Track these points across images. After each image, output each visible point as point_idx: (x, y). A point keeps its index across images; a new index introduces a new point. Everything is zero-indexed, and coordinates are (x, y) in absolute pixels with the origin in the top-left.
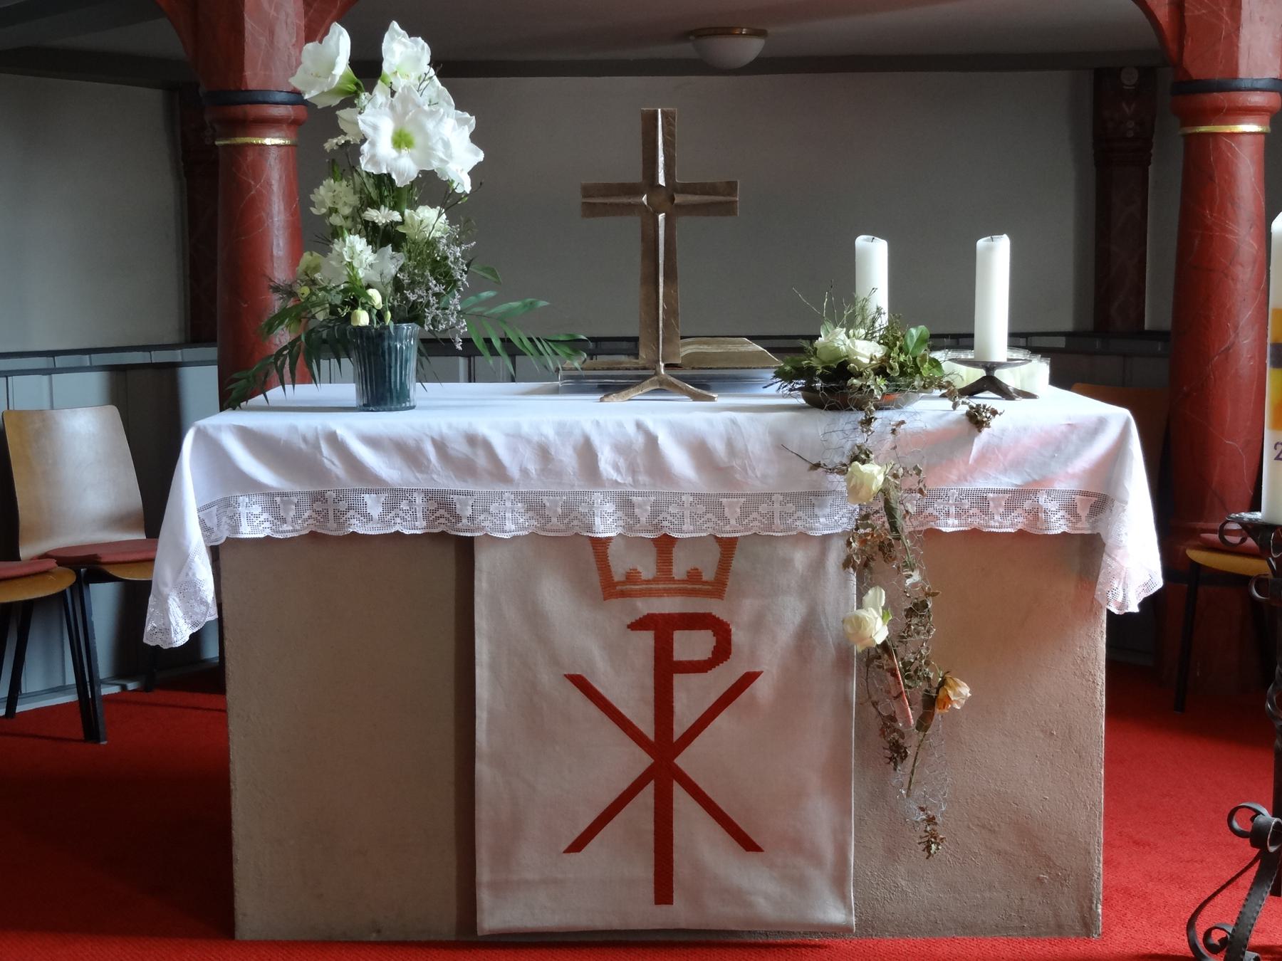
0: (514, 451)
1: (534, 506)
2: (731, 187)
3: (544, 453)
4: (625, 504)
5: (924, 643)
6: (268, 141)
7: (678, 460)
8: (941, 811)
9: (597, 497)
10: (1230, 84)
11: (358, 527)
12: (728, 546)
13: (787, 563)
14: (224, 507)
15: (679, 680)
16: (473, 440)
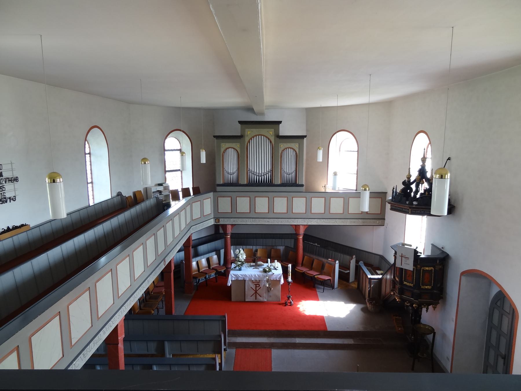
1: (249, 278)
2: (260, 257)
3: (249, 275)
4: (254, 278)
5: (270, 286)
7: (257, 276)
10: (299, 234)
11: (239, 279)
12: (260, 280)
15: (257, 287)
16: (246, 275)
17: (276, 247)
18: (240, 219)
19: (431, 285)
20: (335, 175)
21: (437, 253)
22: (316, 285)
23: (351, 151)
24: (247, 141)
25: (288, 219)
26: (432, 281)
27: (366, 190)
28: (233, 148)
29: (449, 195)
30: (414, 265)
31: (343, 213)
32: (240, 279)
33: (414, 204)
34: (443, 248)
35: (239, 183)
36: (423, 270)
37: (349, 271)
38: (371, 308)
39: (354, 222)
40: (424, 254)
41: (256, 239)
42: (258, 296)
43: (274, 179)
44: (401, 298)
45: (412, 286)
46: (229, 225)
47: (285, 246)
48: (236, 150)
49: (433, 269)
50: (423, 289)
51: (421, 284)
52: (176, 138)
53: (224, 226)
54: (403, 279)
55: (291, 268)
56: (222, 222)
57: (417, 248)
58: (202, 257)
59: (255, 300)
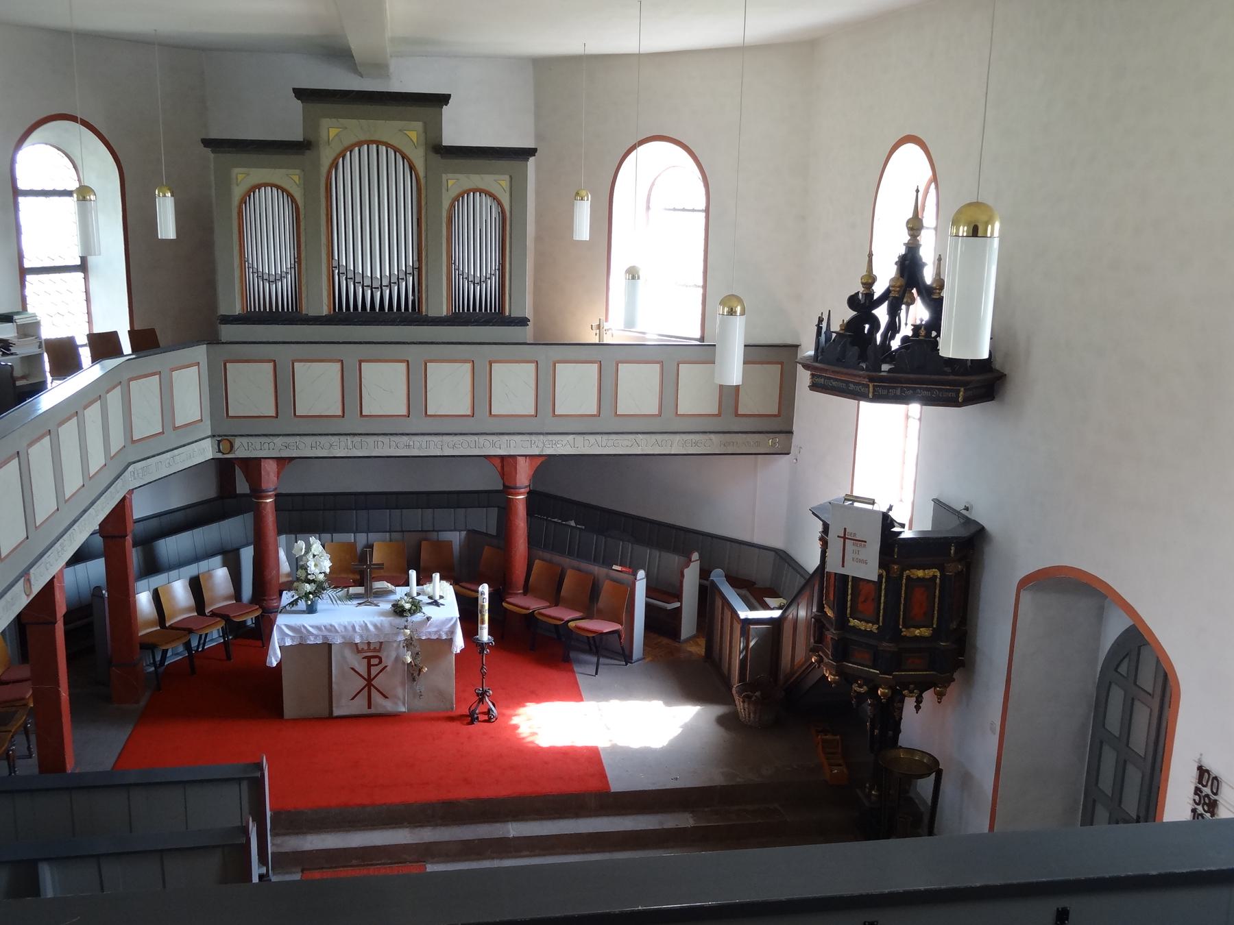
0: (339, 628)
1: (343, 637)
2: (383, 564)
3: (345, 627)
4: (361, 636)
6: (268, 501)
7: (371, 627)
8: (423, 690)
9: (356, 635)
10: (515, 488)
11: (309, 642)
12: (381, 643)
13: (393, 646)
14: (282, 639)
16: (331, 625)
17: (435, 533)
18: (309, 440)
19: (932, 626)
20: (633, 278)
21: (951, 528)
22: (573, 655)
23: (684, 210)
24: (326, 162)
25: (476, 438)
26: (936, 612)
27: (736, 312)
28: (278, 187)
29: (991, 339)
30: (882, 565)
31: (660, 415)
32: (311, 641)
33: (882, 370)
34: (967, 509)
35: (300, 312)
36: (908, 577)
37: (677, 605)
38: (749, 714)
39: (696, 444)
40: (910, 528)
41: (366, 508)
42: (376, 696)
43: (427, 299)
44: (839, 672)
45: (876, 631)
46: (271, 461)
47: (469, 531)
48: (289, 195)
49: (938, 574)
50: (908, 638)
51: (901, 623)
52: (59, 149)
53: (252, 466)
54: (848, 611)
55: (486, 596)
56: (243, 449)
57: (890, 509)
58: (174, 573)
59: (366, 711)
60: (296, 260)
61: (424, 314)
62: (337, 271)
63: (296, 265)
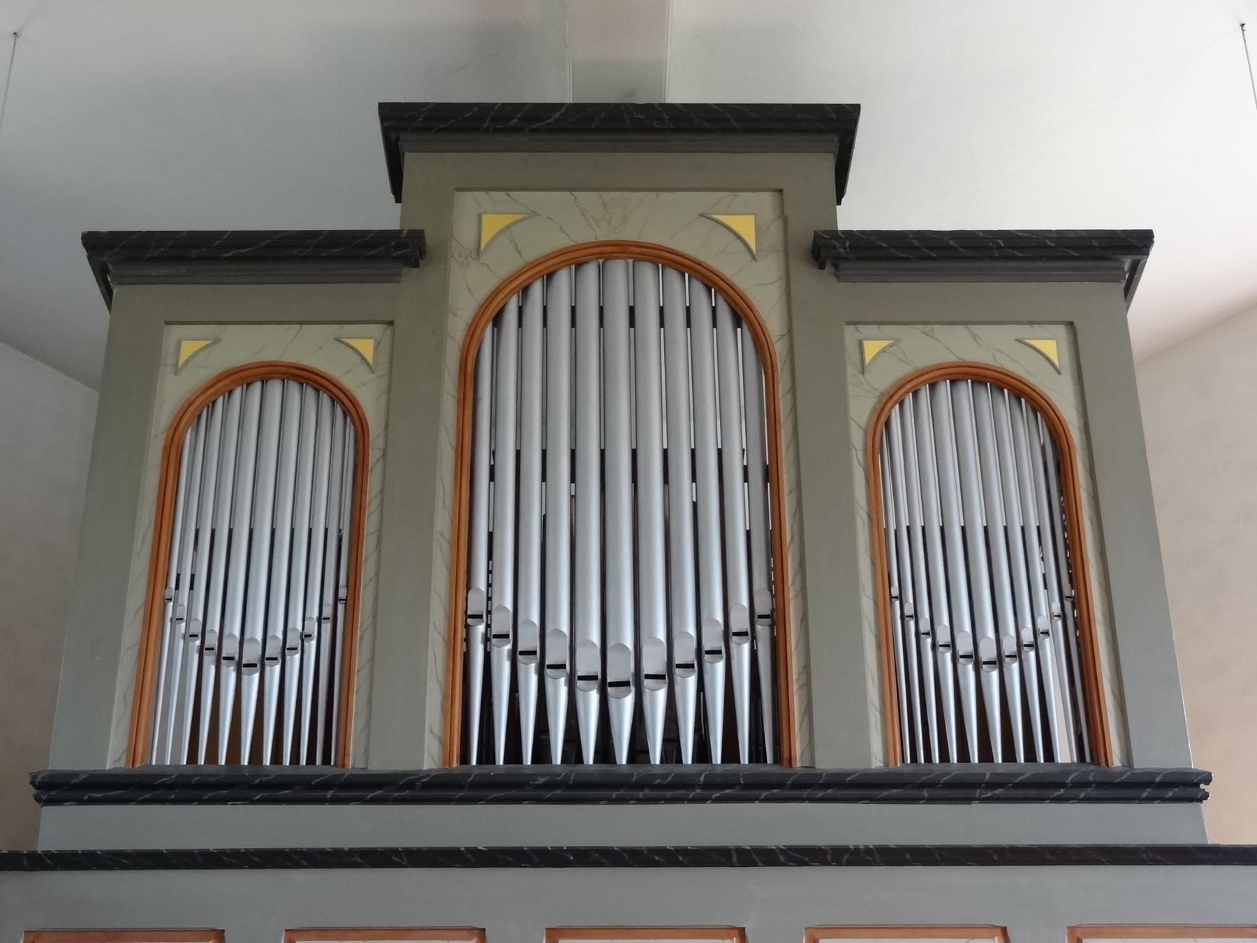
60: (343, 593)
61: (798, 764)
62: (481, 628)
63: (341, 607)
